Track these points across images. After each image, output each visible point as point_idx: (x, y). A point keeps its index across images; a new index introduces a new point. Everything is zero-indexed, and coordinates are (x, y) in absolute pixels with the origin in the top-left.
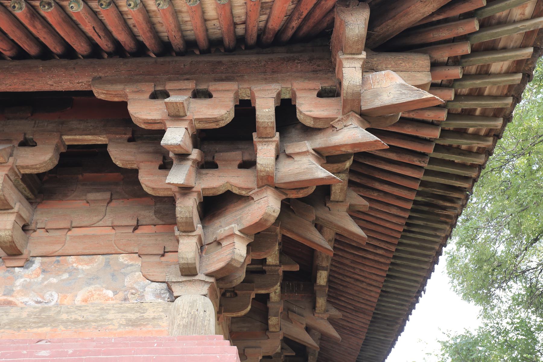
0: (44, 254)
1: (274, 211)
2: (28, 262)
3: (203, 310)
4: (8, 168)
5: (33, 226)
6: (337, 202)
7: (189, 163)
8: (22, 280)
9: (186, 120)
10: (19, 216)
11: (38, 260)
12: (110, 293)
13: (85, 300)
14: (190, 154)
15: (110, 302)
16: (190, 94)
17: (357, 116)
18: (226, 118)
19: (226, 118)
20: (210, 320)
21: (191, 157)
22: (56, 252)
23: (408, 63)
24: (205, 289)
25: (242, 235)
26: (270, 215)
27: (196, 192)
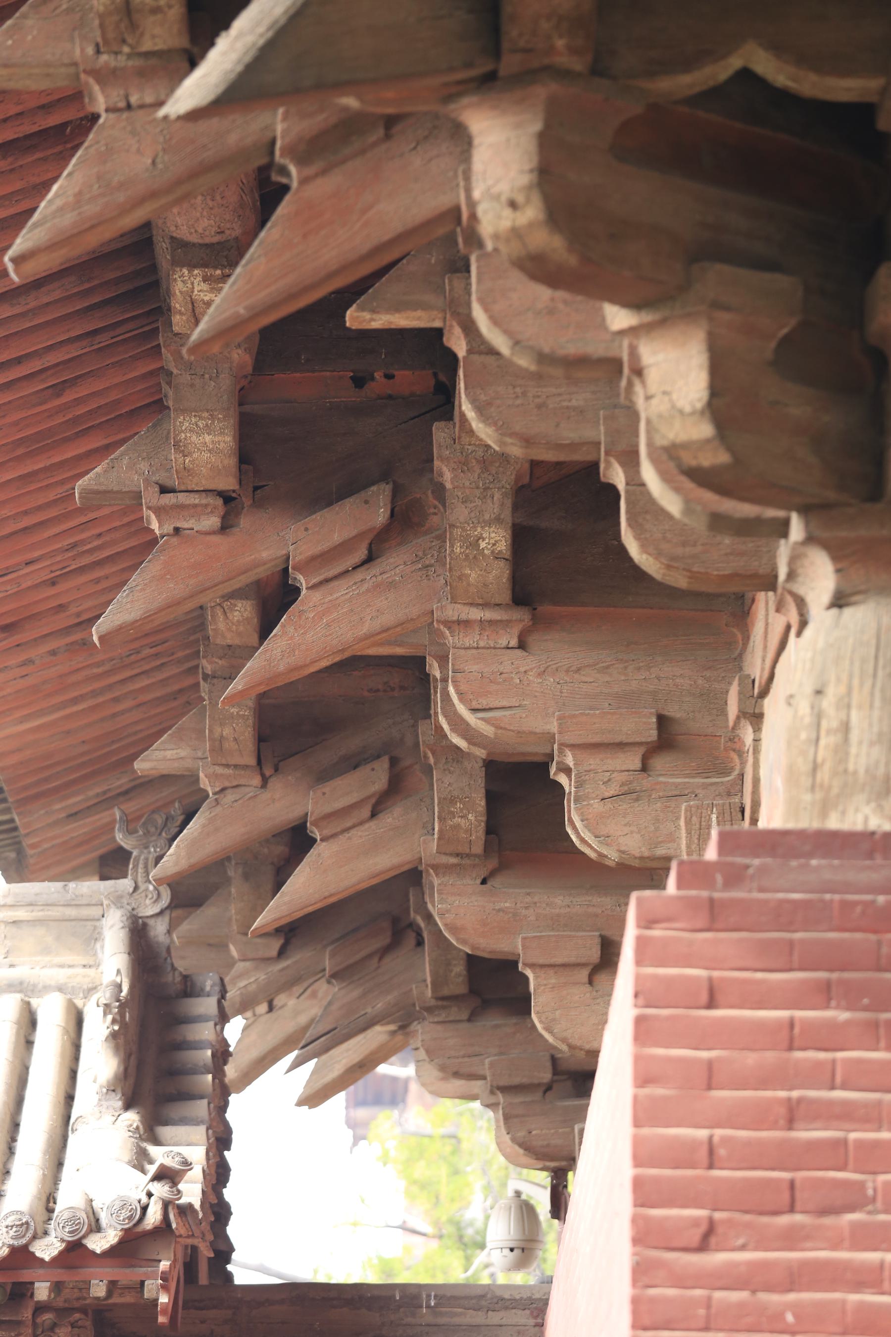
1: (513, 205)
3: (809, 689)
20: (846, 728)
25: (647, 317)
26: (516, 232)
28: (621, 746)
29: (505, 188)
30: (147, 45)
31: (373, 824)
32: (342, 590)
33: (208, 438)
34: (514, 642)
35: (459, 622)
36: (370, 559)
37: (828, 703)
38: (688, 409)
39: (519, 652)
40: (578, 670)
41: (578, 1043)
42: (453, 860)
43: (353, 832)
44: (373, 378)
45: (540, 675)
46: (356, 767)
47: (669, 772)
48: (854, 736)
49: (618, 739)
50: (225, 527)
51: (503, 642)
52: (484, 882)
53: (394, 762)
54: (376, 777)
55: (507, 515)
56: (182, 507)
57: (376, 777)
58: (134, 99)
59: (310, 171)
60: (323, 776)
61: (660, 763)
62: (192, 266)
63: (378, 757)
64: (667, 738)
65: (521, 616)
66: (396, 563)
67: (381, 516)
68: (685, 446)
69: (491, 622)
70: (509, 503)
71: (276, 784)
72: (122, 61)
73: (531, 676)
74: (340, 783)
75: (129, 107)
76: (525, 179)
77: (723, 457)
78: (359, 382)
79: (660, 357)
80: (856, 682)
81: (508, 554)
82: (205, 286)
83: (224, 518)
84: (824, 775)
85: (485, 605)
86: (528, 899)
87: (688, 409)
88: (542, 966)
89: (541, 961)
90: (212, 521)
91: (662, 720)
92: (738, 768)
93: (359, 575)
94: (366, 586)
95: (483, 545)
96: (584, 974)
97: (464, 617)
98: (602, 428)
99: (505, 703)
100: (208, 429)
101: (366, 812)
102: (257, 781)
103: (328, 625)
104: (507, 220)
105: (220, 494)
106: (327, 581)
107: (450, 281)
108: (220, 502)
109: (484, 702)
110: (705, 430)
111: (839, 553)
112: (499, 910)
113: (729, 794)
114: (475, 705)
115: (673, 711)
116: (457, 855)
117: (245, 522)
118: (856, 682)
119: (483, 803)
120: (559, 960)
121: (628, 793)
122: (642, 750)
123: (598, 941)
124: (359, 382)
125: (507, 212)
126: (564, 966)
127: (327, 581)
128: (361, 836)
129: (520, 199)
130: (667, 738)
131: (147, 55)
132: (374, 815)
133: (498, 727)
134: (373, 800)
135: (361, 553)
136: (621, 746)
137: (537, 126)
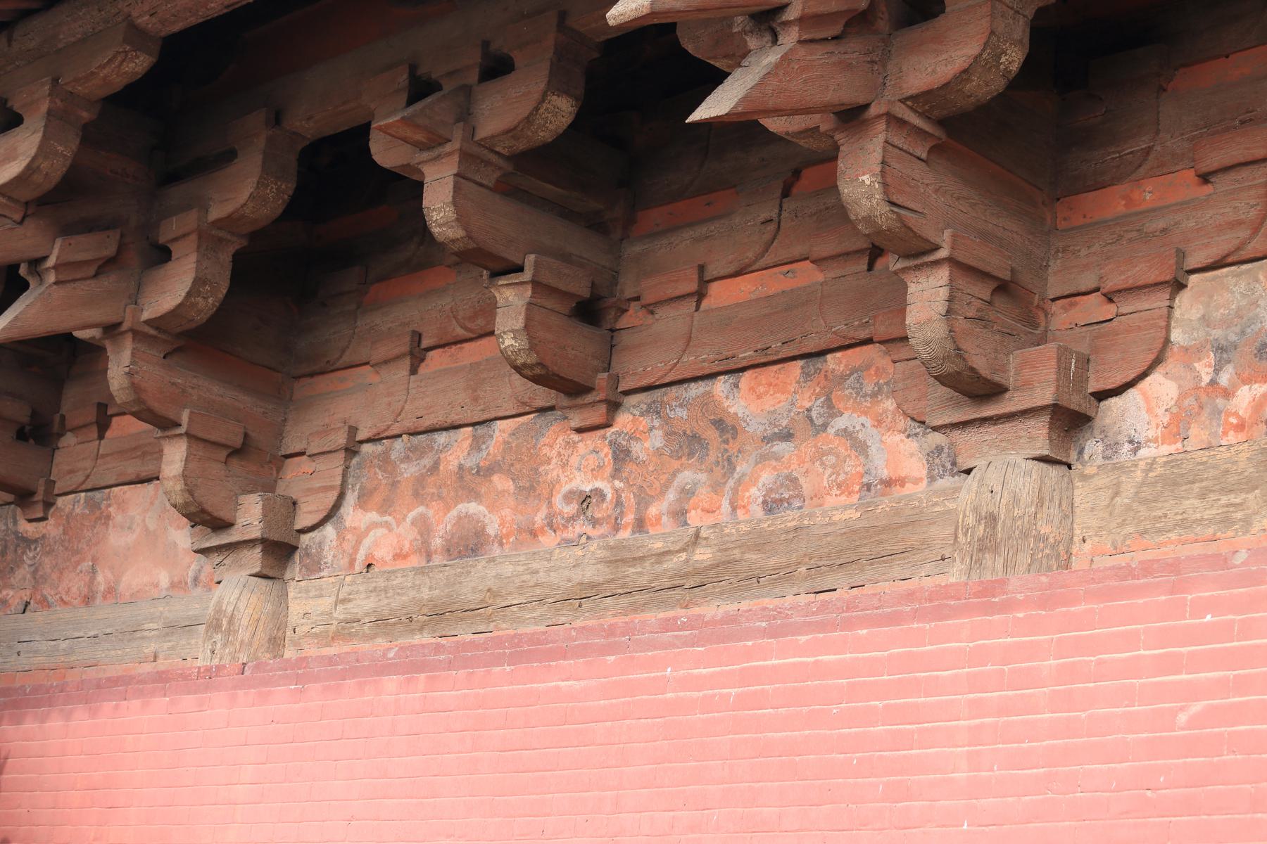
31: (92, 282)
32: (818, 54)
40: (958, 199)
41: (210, 509)
42: (152, 332)
43: (77, 284)
45: (936, 191)
46: (90, 231)
47: (1004, 313)
49: (988, 269)
53: (122, 236)
54: (105, 245)
55: (1026, 40)
60: (67, 230)
63: (108, 228)
66: (854, 49)
71: (30, 224)
73: (930, 190)
74: (82, 240)
86: (195, 381)
89: (200, 435)
92: (1043, 324)
93: (830, 47)
94: (834, 59)
95: (1003, 59)
96: (225, 453)
97: (906, 118)
99: (912, 206)
101: (92, 270)
102: (17, 217)
103: (805, 82)
109: (900, 200)
112: (173, 384)
114: (894, 199)
119: (225, 292)
120: (213, 438)
128: (83, 289)
132: (96, 276)
134: (100, 263)
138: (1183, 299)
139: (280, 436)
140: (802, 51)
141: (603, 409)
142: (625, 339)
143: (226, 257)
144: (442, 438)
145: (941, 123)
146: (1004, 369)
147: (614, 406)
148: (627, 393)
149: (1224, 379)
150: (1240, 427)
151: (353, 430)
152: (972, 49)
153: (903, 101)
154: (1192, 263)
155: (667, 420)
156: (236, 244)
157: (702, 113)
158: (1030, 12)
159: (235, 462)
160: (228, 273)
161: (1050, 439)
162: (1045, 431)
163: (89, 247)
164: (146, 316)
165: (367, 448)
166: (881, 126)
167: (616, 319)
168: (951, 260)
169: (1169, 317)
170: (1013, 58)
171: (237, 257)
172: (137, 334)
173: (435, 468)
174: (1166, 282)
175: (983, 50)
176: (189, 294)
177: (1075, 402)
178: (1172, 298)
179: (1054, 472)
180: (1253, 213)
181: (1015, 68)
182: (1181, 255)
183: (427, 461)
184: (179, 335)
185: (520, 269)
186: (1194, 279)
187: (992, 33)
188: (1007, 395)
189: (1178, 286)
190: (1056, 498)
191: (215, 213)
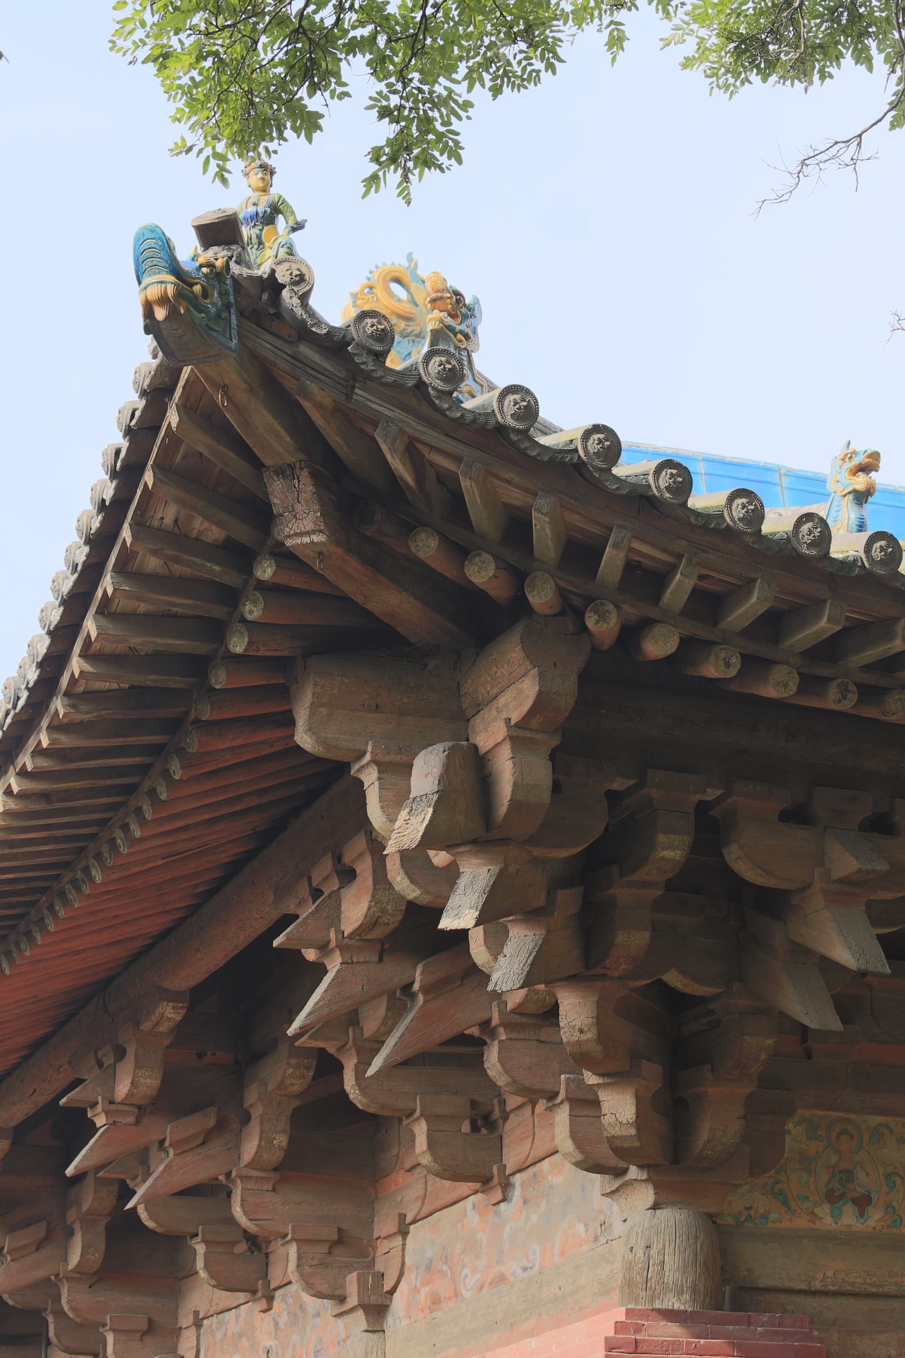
0: (518, 1167)
1: (581, 1031)
2: (506, 1186)
3: (643, 1245)
4: (354, 1052)
5: (497, 1113)
6: (803, 889)
7: (421, 998)
8: (508, 1227)
9: (332, 950)
10: (431, 1118)
11: (517, 1179)
12: (580, 1228)
13: (563, 1253)
14: (413, 983)
15: (585, 1248)
16: (335, 884)
17: (462, 849)
18: (384, 911)
19: (384, 911)
20: (663, 1263)
21: (416, 986)
22: (528, 1157)
23: (502, 666)
24: (646, 1195)
25: (606, 1080)
26: (578, 1042)
27: (499, 1025)
28: (320, 1241)
29: (578, 1023)
30: (369, 937)
33: (149, 1081)
34: (270, 1188)
35: (246, 1177)
36: (203, 1143)
37: (653, 1252)
38: (625, 1122)
39: (273, 1193)
40: (300, 1204)
42: (77, 1275)
44: (206, 1054)
45: (282, 1204)
46: (28, 1225)
48: (667, 1268)
49: (320, 1238)
50: (137, 1122)
51: (265, 1188)
52: (90, 1287)
53: (48, 1223)
54: (39, 1231)
56: (118, 1112)
57: (39, 1231)
58: (355, 959)
59: (429, 997)
61: (337, 1250)
62: (169, 1001)
63: (40, 1221)
64: (341, 1240)
65: (276, 1176)
67: (212, 1122)
68: (618, 1138)
69: (262, 1178)
70: (288, 1122)
72: (353, 942)
75: (352, 963)
76: (590, 1021)
77: (637, 1144)
78: (200, 1056)
79: (610, 1098)
80: (667, 1244)
81: (285, 1148)
82: (171, 1011)
83: (137, 1118)
84: (652, 1283)
85: (260, 1170)
87: (625, 1122)
88: (119, 1331)
90: (131, 1119)
91: (340, 1231)
95: (275, 1142)
96: (138, 1335)
97: (249, 1174)
98: (418, 1103)
100: (150, 1077)
101: (33, 1248)
104: (576, 1036)
105: (139, 1107)
106: (184, 1152)
107: (354, 1030)
108: (137, 1110)
109: (256, 1216)
110: (633, 1131)
111: (658, 1188)
113: (368, 1267)
114: (252, 1217)
115: (344, 1226)
116: (79, 1273)
117: (145, 1120)
118: (667, 1244)
121: (322, 1264)
122: (330, 1243)
123: (146, 1320)
124: (200, 1056)
125: (577, 1034)
126: (130, 1331)
127: (184, 1152)
129: (586, 1029)
130: (341, 1240)
131: (367, 940)
132: (37, 1250)
133: (262, 1228)
135: (200, 1141)
136: (320, 1241)
137: (596, 998)
138: (409, 1238)
139: (175, 1316)
140: (178, 1159)
141: (264, 1301)
142: (272, 1258)
143: (100, 1229)
144: (227, 1314)
145: (275, 1169)
146: (343, 1286)
147: (270, 1299)
148: (276, 1289)
149: (418, 1285)
150: (422, 1310)
151: (196, 1313)
152: (256, 1142)
153: (246, 1166)
154: (408, 1221)
155: (287, 1303)
156: (104, 1222)
157: (127, 1207)
158: (289, 1111)
159: (148, 1340)
160: (104, 1238)
161: (367, 1321)
162: (364, 1317)
163: (26, 1237)
164: (70, 1267)
165: (206, 1322)
166: (239, 1181)
167: (267, 1247)
168: (293, 1239)
169: (403, 1249)
170: (281, 1140)
171: (107, 1228)
172: (68, 1279)
173: (225, 1334)
174: (395, 1234)
175: (260, 1142)
176: (82, 1255)
177: (374, 1300)
178: (404, 1239)
179: (375, 1336)
180: (421, 1193)
181: (284, 1144)
182: (402, 1217)
183: (223, 1330)
184: (94, 1274)
185: (197, 1235)
186: (412, 1227)
187: (262, 1132)
188: (348, 1299)
189: (404, 1233)
190: (375, 1350)
191: (85, 1208)
